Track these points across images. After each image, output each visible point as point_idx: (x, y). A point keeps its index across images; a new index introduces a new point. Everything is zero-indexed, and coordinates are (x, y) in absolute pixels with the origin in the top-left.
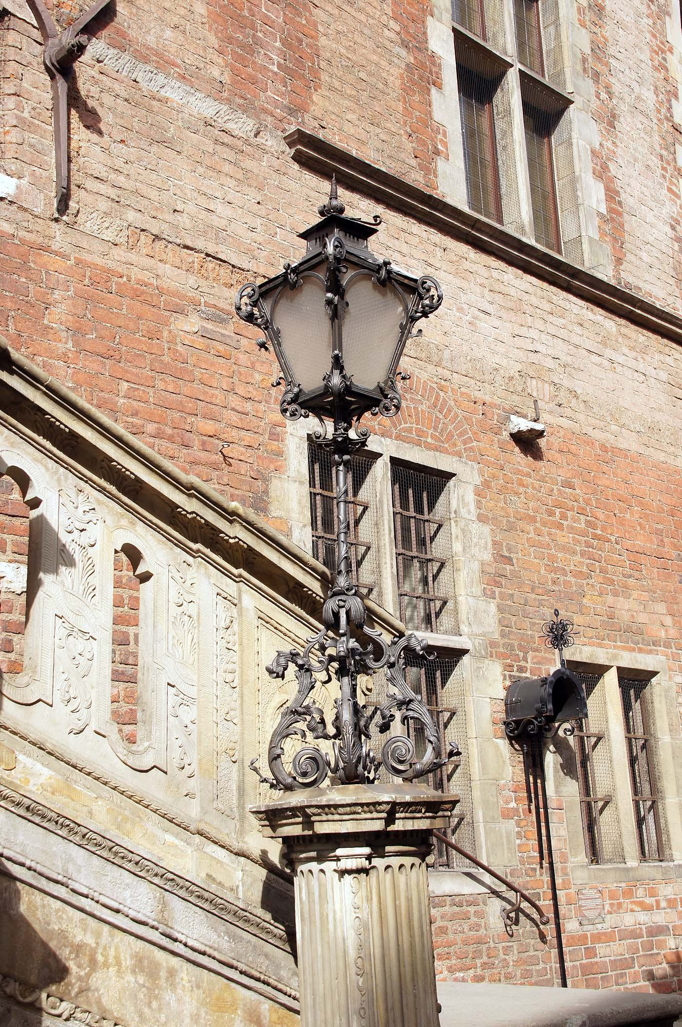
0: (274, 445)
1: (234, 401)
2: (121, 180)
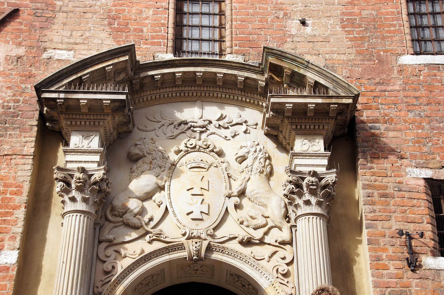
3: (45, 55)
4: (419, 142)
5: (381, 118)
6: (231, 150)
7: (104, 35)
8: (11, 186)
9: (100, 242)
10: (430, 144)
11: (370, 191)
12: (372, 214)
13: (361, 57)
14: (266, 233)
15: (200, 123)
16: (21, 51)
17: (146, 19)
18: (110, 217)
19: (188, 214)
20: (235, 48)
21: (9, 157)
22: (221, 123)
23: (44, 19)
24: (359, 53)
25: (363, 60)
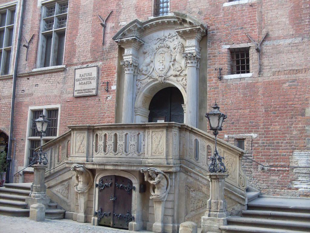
0: (307, 102)
1: (297, 96)
2: (271, 64)
3: (119, 25)
5: (215, 29)
6: (172, 45)
7: (134, 14)
8: (113, 67)
9: (137, 80)
10: (230, 36)
12: (210, 63)
14: (181, 73)
15: (163, 38)
16: (114, 25)
17: (146, 5)
18: (139, 73)
19: (159, 69)
20: (171, 10)
21: (112, 59)
22: (169, 37)
23: (119, 13)
24: (210, 5)
25: (211, 7)
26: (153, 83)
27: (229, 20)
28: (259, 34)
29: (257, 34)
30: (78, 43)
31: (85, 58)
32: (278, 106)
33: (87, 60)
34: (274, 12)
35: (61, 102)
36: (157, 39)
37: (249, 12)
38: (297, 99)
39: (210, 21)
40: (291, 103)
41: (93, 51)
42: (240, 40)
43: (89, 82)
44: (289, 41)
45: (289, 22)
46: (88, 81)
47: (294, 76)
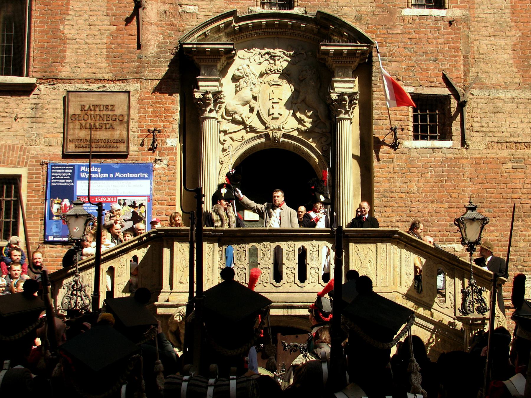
2: (484, 129)
4: (408, 69)
9: (220, 132)
11: (378, 101)
13: (379, 10)
16: (166, 7)
26: (258, 141)
27: (414, 41)
28: (465, 75)
29: (460, 74)
30: (73, 32)
31: (94, 70)
32: (496, 200)
33: (99, 76)
34: (491, 41)
35: (26, 163)
36: (265, 55)
37: (449, 34)
38: (525, 191)
39: (378, 37)
40: (516, 196)
41: (113, 57)
42: (431, 80)
43: (108, 126)
44: (515, 94)
45: (514, 61)
46: (105, 122)
47: (519, 153)
